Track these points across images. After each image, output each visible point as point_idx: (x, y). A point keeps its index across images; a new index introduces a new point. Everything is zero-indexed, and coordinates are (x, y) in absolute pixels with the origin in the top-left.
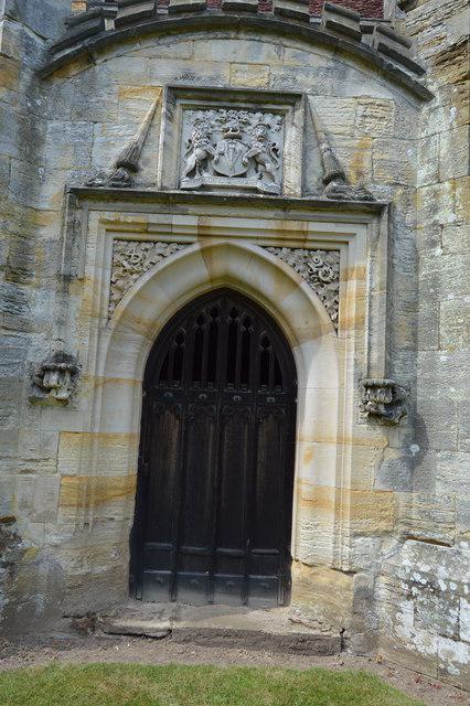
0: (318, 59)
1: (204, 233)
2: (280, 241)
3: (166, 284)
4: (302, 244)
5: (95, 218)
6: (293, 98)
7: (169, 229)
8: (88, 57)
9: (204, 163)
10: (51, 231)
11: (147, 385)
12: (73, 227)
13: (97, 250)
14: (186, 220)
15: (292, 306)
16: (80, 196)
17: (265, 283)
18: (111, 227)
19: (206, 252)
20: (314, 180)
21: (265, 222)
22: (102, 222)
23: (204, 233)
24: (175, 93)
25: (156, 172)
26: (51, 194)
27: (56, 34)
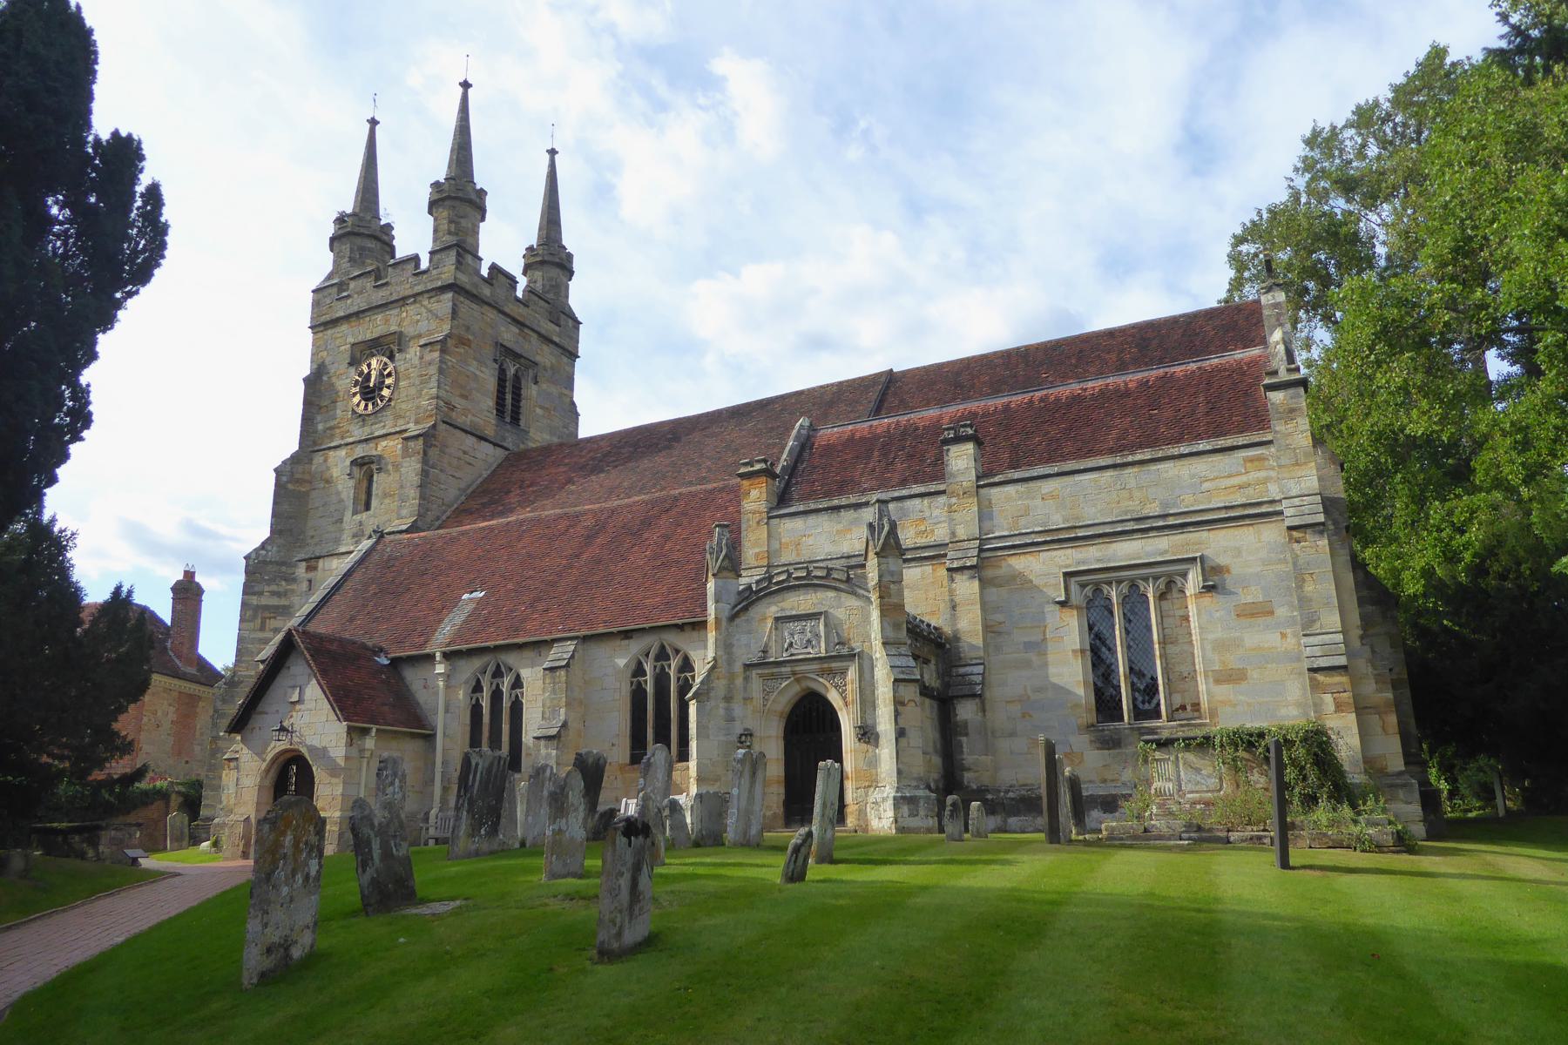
0: (831, 594)
2: (822, 673)
3: (785, 694)
4: (831, 673)
5: (754, 673)
7: (780, 674)
8: (746, 609)
9: (791, 645)
10: (739, 681)
11: (785, 738)
12: (746, 679)
13: (756, 685)
14: (786, 669)
15: (833, 697)
16: (748, 667)
18: (761, 676)
21: (815, 666)
23: (794, 673)
24: (777, 619)
26: (738, 668)
27: (733, 601)
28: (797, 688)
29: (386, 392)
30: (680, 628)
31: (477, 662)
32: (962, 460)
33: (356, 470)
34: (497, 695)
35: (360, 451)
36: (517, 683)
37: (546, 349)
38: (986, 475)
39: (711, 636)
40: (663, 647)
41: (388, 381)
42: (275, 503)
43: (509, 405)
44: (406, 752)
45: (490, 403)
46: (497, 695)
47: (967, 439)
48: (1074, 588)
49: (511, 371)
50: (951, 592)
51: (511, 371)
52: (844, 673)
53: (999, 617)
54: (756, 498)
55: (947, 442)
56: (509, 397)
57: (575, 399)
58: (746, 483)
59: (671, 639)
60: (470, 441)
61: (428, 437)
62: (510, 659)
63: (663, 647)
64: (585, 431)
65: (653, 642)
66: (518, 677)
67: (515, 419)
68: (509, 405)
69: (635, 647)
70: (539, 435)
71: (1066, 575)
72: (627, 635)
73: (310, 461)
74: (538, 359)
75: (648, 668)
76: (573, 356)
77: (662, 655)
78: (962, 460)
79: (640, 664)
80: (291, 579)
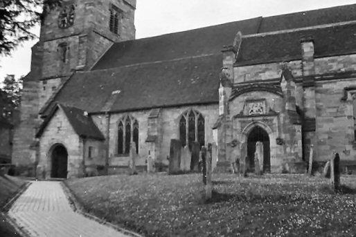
1: (253, 120)
2: (264, 120)
3: (248, 128)
5: (238, 120)
6: (264, 99)
9: (252, 111)
14: (250, 119)
15: (268, 129)
16: (236, 117)
17: (263, 127)
18: (240, 121)
19: (254, 123)
20: (268, 111)
21: (261, 118)
22: (240, 121)
23: (253, 120)
25: (245, 113)
28: (253, 126)
29: (71, 20)
30: (199, 104)
31: (121, 116)
32: (308, 48)
33: (60, 48)
34: (128, 127)
35: (60, 41)
36: (136, 123)
37: (126, 6)
38: (319, 53)
39: (222, 106)
40: (192, 112)
41: (72, 16)
42: (32, 59)
43: (114, 25)
44: (95, 145)
45: (108, 25)
46: (128, 127)
47: (310, 41)
48: (349, 95)
49: (115, 13)
50: (304, 95)
51: (115, 13)
52: (272, 120)
53: (321, 104)
54: (229, 61)
55: (302, 42)
56: (114, 24)
57: (135, 24)
58: (224, 54)
59: (195, 108)
60: (102, 38)
61: (88, 36)
62: (134, 114)
63: (192, 112)
64: (138, 36)
65: (188, 109)
66: (136, 120)
67: (116, 32)
68: (114, 25)
69: (181, 111)
70: (124, 38)
71: (347, 89)
72: (179, 106)
73: (43, 45)
74: (124, 10)
75: (187, 118)
76: (134, 8)
77: (192, 114)
78: (308, 48)
79: (183, 117)
80: (38, 87)
